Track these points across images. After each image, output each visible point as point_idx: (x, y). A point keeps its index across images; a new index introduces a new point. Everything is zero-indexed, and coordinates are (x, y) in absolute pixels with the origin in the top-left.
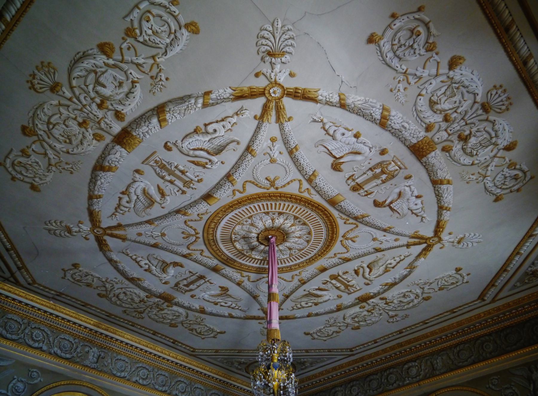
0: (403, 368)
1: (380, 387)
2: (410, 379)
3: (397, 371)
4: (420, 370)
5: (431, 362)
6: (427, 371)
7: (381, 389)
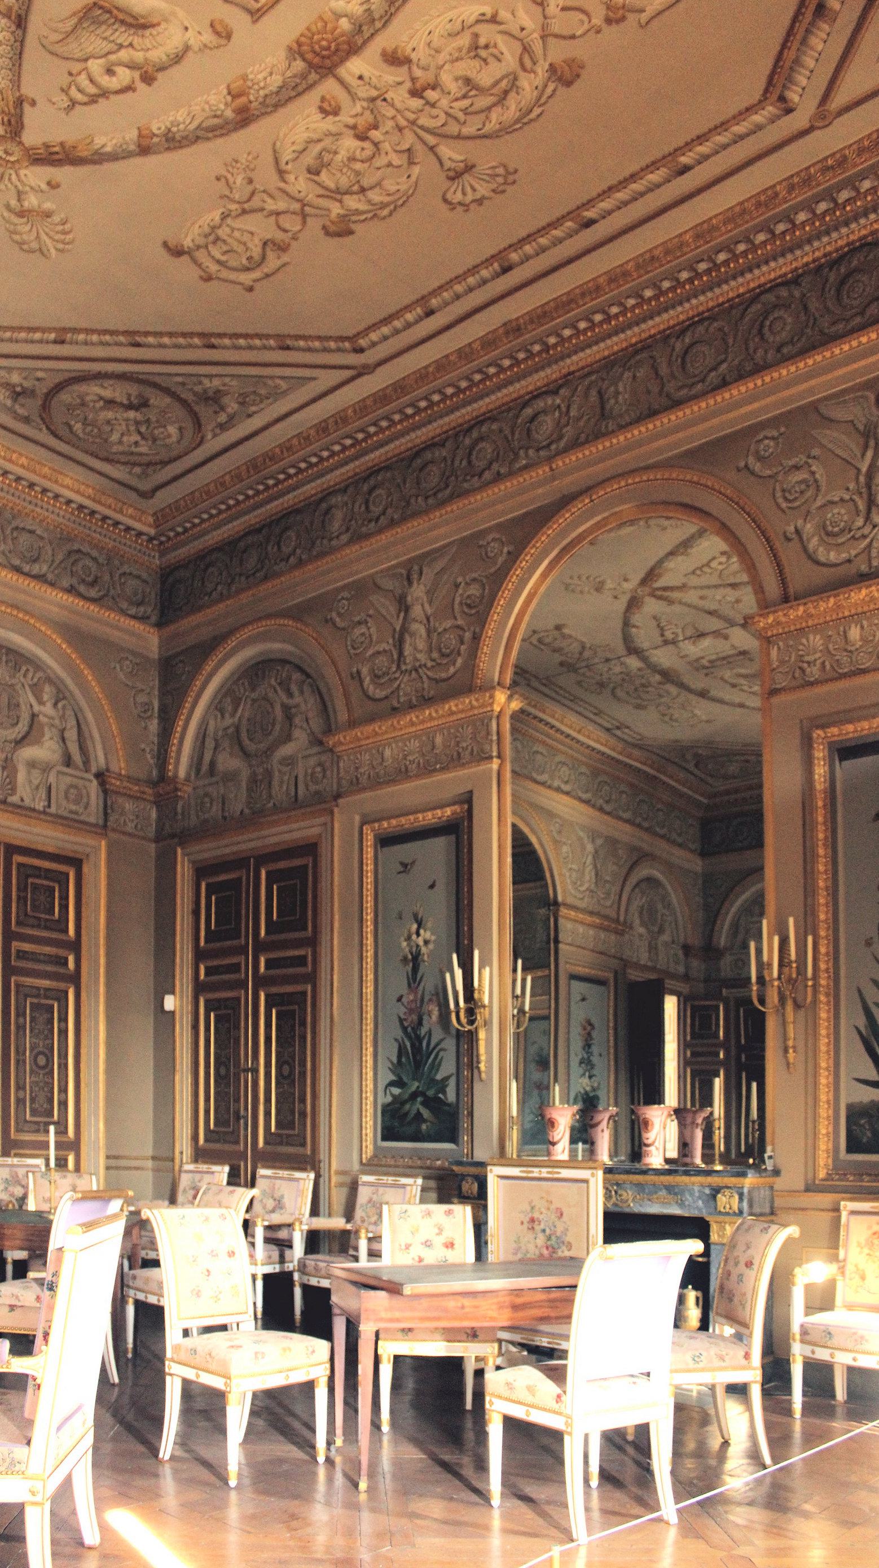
0: (517, 417)
1: (447, 486)
2: (531, 452)
3: (501, 431)
4: (563, 421)
5: (600, 394)
6: (582, 423)
7: (448, 492)
